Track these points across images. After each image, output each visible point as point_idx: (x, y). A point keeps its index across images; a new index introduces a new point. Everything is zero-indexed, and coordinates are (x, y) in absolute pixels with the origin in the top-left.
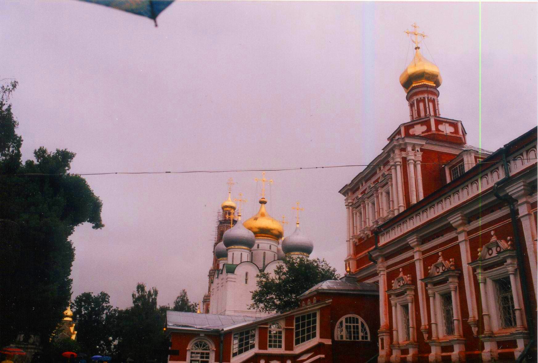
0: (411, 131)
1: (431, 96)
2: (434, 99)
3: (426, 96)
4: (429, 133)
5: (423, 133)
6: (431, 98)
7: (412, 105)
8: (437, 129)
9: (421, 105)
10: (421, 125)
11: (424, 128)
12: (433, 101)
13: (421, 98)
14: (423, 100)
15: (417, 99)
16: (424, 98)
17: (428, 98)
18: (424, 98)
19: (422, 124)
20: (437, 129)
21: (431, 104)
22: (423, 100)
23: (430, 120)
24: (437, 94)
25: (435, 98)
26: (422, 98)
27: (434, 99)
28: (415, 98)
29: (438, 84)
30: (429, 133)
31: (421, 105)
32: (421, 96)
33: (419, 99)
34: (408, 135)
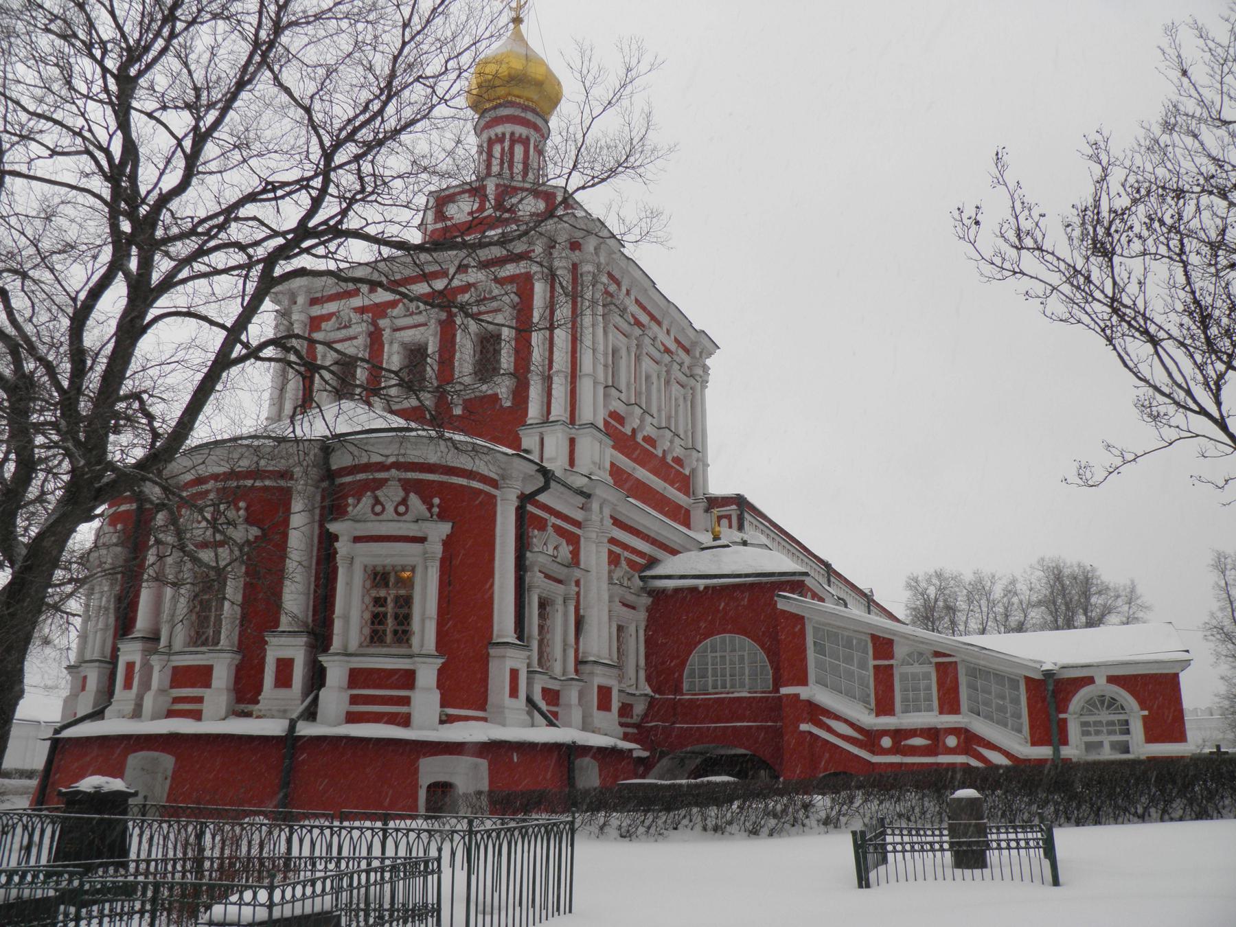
3: (534, 136)
13: (521, 135)
14: (525, 142)
15: (512, 134)
18: (528, 139)
26: (524, 137)
28: (507, 128)
31: (519, 150)
32: (520, 130)
33: (517, 135)
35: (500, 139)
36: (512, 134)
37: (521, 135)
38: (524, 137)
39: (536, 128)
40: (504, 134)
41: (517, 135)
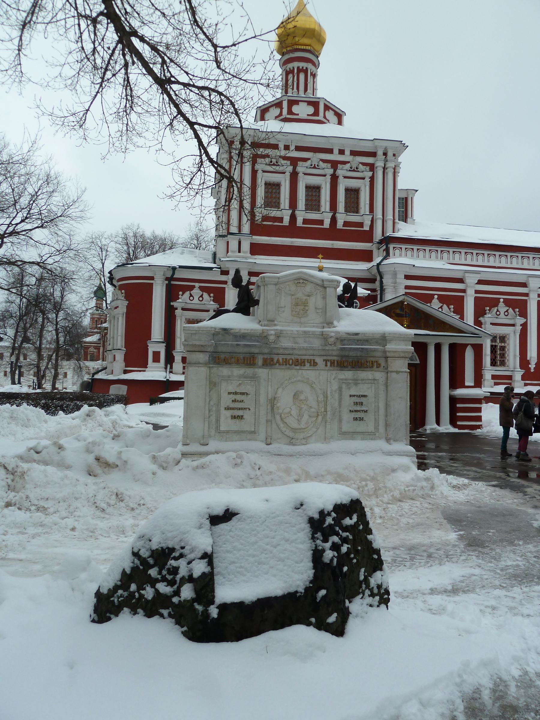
0: (295, 109)
1: (313, 68)
3: (310, 66)
5: (308, 115)
7: (288, 73)
8: (325, 117)
9: (302, 76)
10: (308, 105)
11: (311, 110)
12: (314, 76)
13: (303, 67)
14: (305, 71)
15: (298, 68)
16: (307, 68)
18: (307, 68)
19: (310, 103)
20: (325, 117)
22: (305, 71)
23: (318, 102)
26: (304, 68)
28: (296, 64)
31: (302, 76)
33: (301, 68)
34: (290, 112)
35: (292, 71)
36: (298, 68)
37: (303, 67)
38: (304, 68)
39: (314, 64)
40: (293, 68)
41: (301, 68)
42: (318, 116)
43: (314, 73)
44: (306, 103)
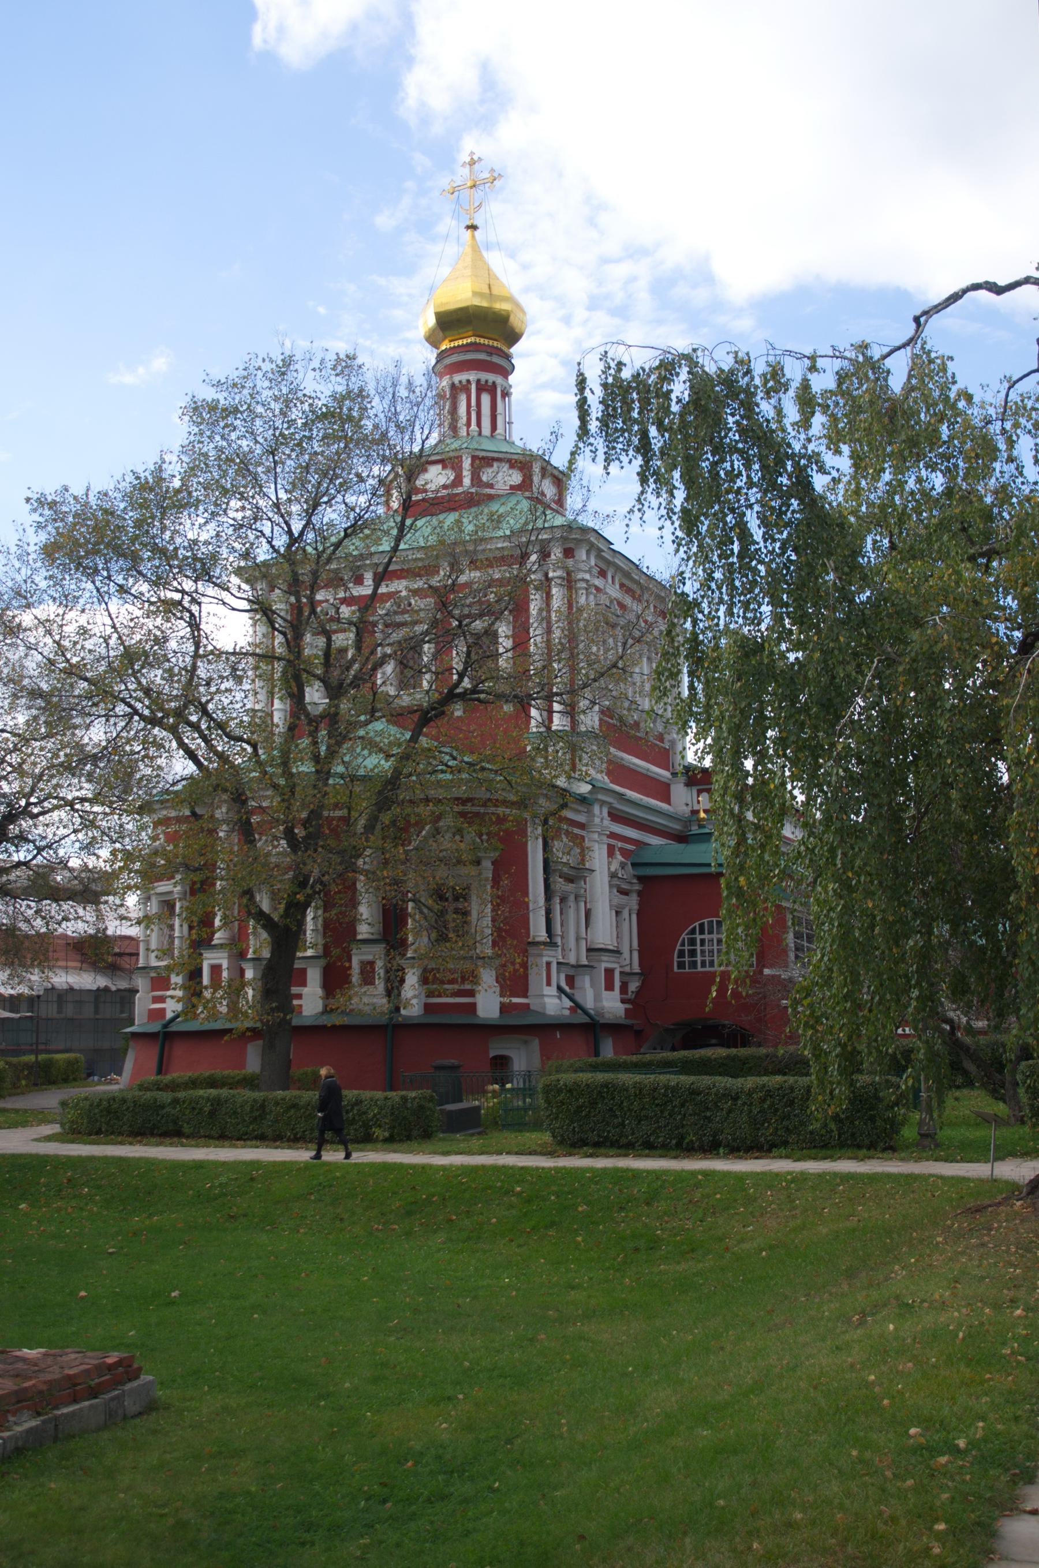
2: (494, 383)
3: (472, 376)
4: (460, 490)
6: (487, 381)
9: (463, 398)
11: (450, 475)
14: (465, 388)
16: (468, 381)
17: (478, 381)
19: (443, 463)
21: (486, 399)
24: (506, 371)
25: (499, 380)
26: (464, 382)
27: (494, 383)
29: (513, 337)
30: (460, 490)
31: (463, 398)
38: (464, 382)
42: (462, 485)
43: (490, 383)
44: (440, 467)
